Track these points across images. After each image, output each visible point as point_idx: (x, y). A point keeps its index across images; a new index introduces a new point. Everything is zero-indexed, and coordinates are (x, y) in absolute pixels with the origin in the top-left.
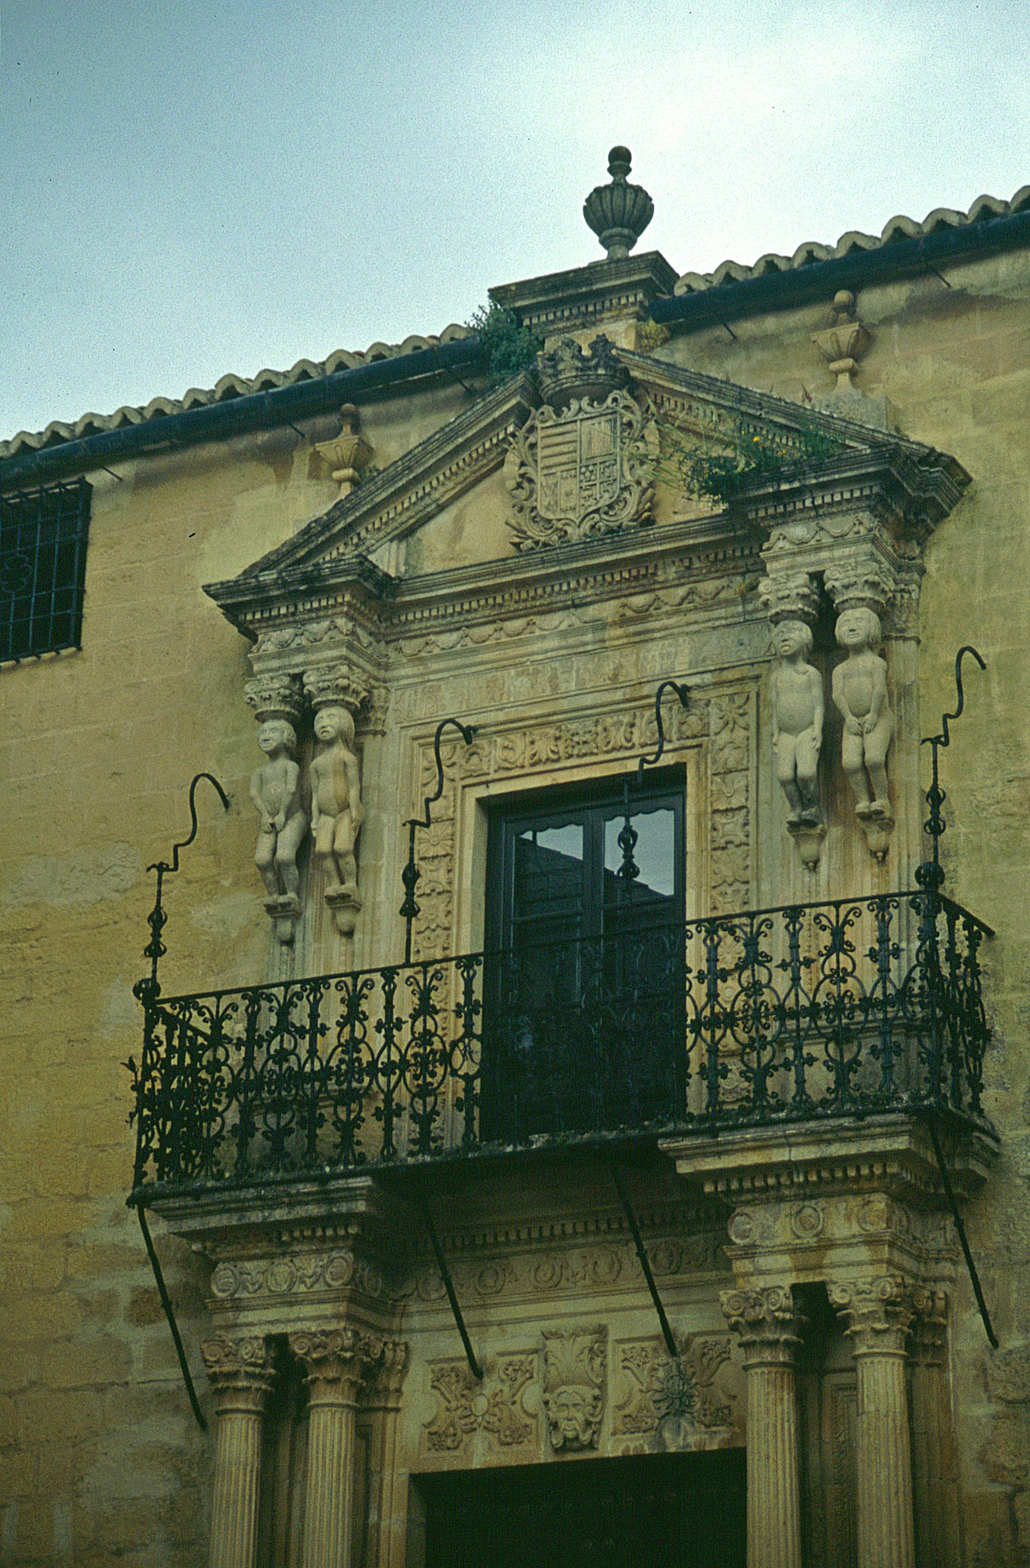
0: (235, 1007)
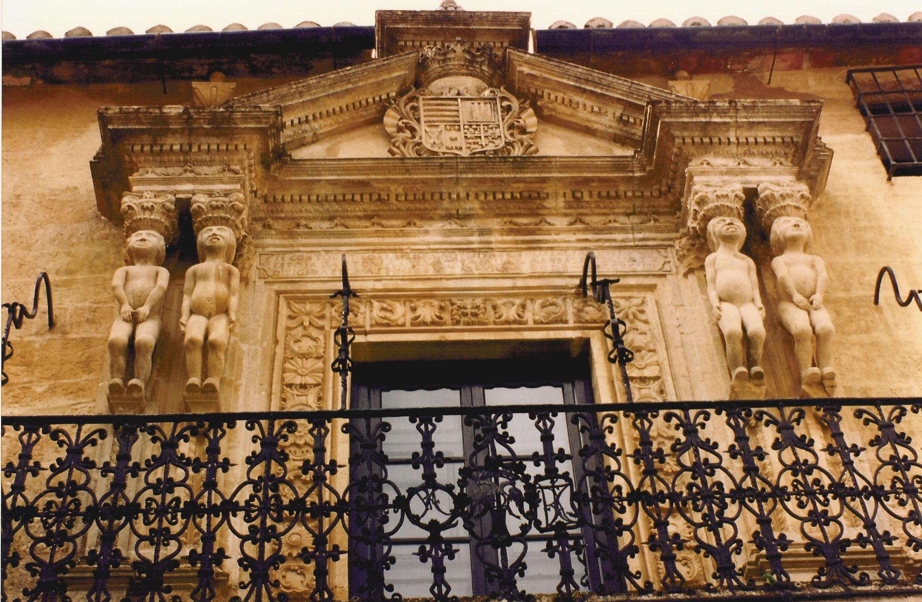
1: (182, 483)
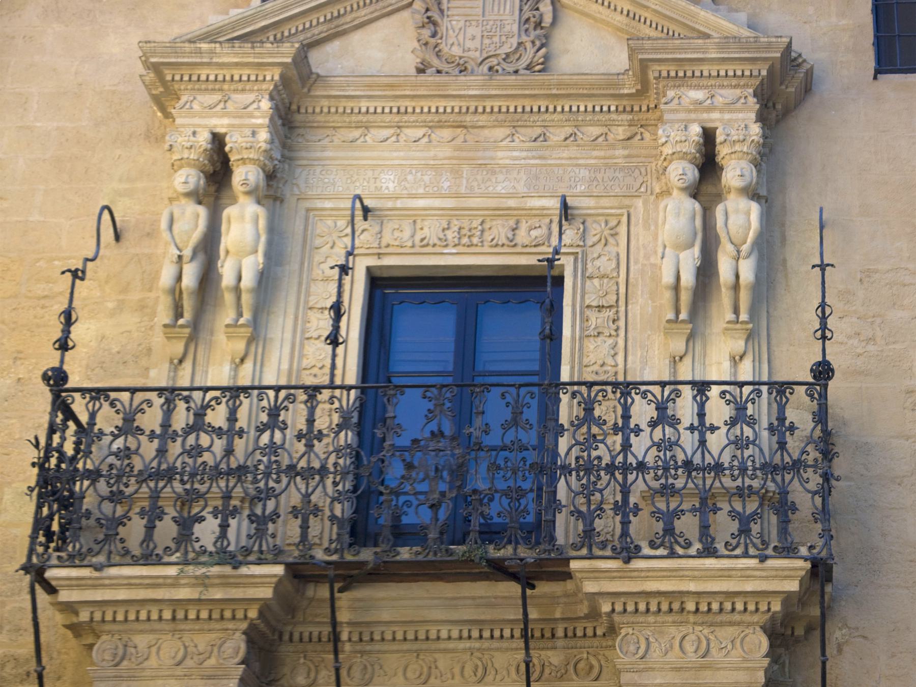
1: (209, 449)
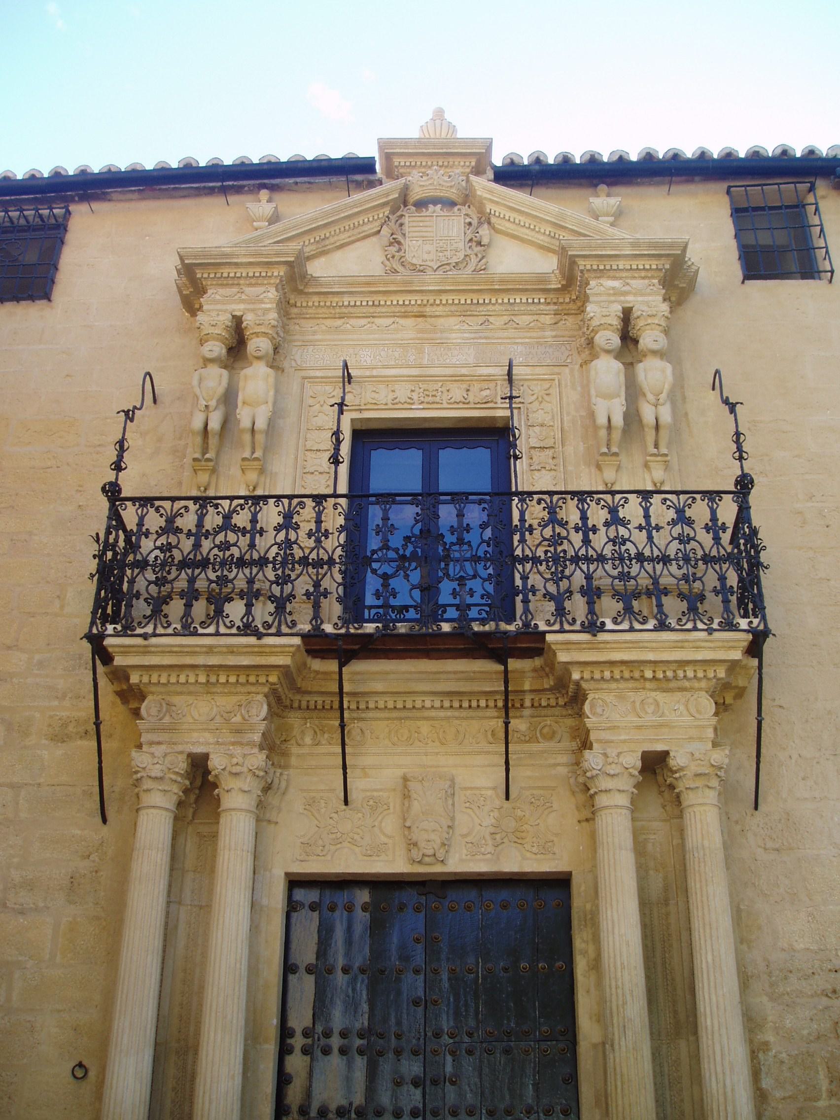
0: (186, 508)
1: (235, 545)
